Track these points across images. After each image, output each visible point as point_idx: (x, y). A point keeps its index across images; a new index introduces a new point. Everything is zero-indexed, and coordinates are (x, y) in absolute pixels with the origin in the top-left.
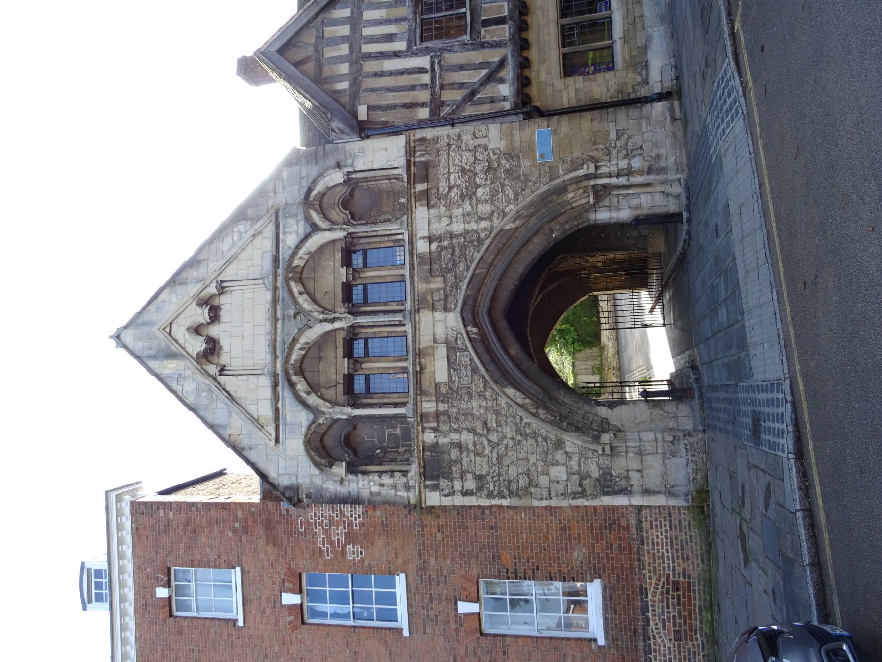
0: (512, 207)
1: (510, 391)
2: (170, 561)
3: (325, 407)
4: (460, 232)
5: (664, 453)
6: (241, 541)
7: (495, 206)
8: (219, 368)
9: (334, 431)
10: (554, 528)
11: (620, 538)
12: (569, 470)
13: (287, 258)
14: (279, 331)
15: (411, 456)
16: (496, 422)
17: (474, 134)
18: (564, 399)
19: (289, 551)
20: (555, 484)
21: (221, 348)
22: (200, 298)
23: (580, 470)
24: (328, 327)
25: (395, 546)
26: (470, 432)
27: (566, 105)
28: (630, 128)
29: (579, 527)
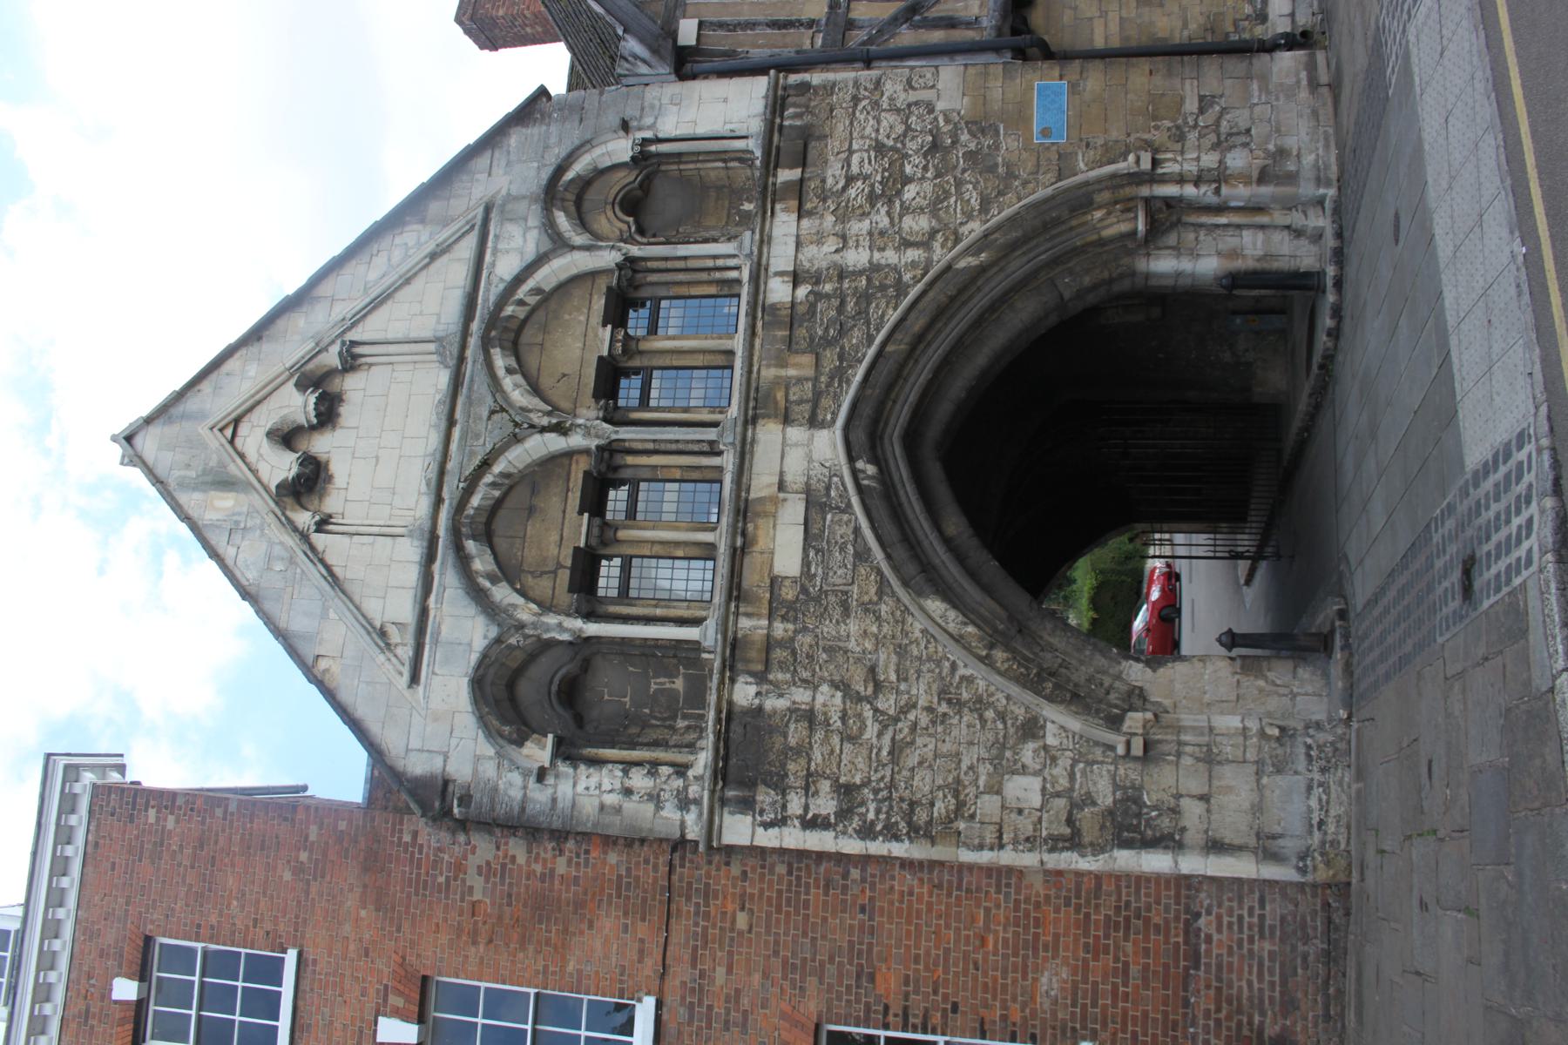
1: (935, 606)
2: (152, 922)
3: (526, 612)
4: (859, 267)
5: (1259, 763)
6: (307, 893)
7: (939, 220)
8: (317, 518)
9: (541, 670)
10: (1002, 920)
11: (1146, 951)
12: (1048, 786)
13: (492, 299)
14: (454, 446)
15: (700, 738)
16: (897, 671)
17: (909, 82)
18: (1052, 640)
19: (406, 926)
20: (1013, 816)
21: (330, 478)
22: (303, 374)
23: (1072, 789)
24: (555, 443)
25: (640, 936)
26: (837, 688)
27: (1099, 43)
28: (1227, 93)
29: (1057, 921)
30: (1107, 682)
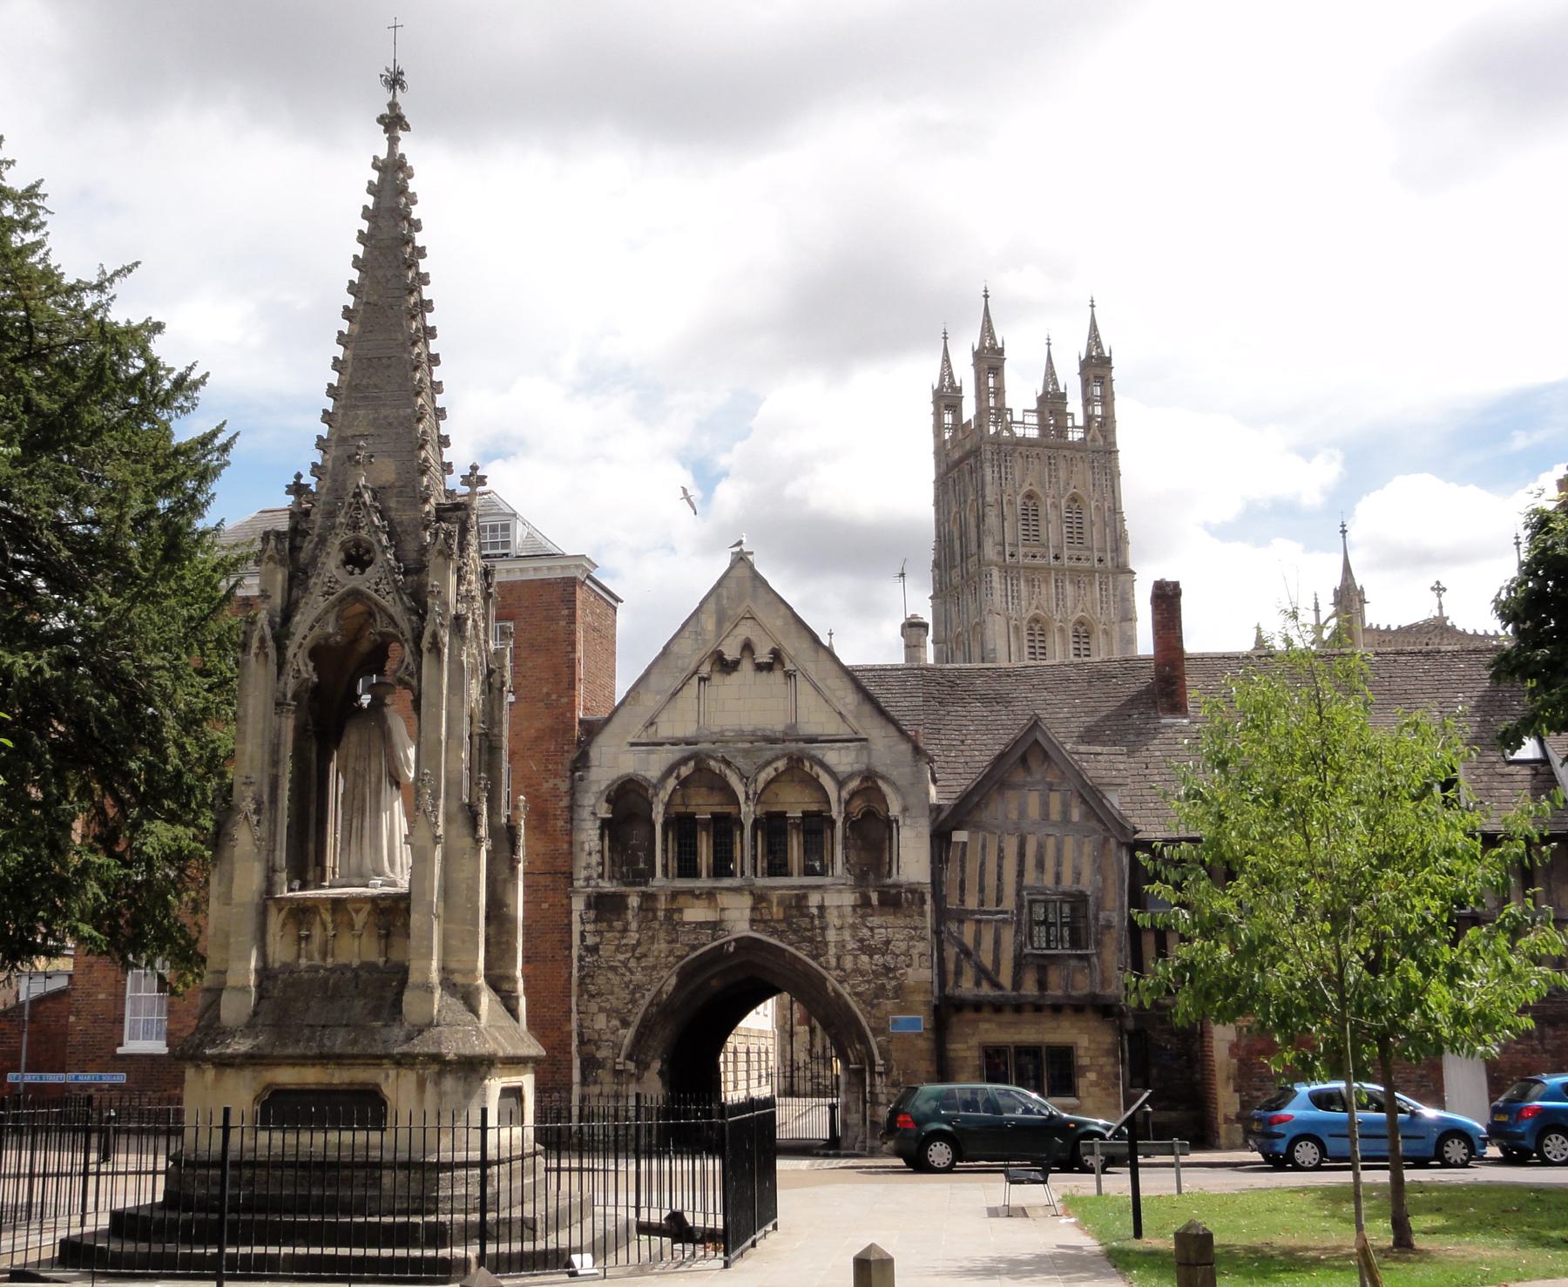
0: (848, 989)
1: (673, 980)
3: (664, 795)
21: (729, 673)
30: (651, 1053)
